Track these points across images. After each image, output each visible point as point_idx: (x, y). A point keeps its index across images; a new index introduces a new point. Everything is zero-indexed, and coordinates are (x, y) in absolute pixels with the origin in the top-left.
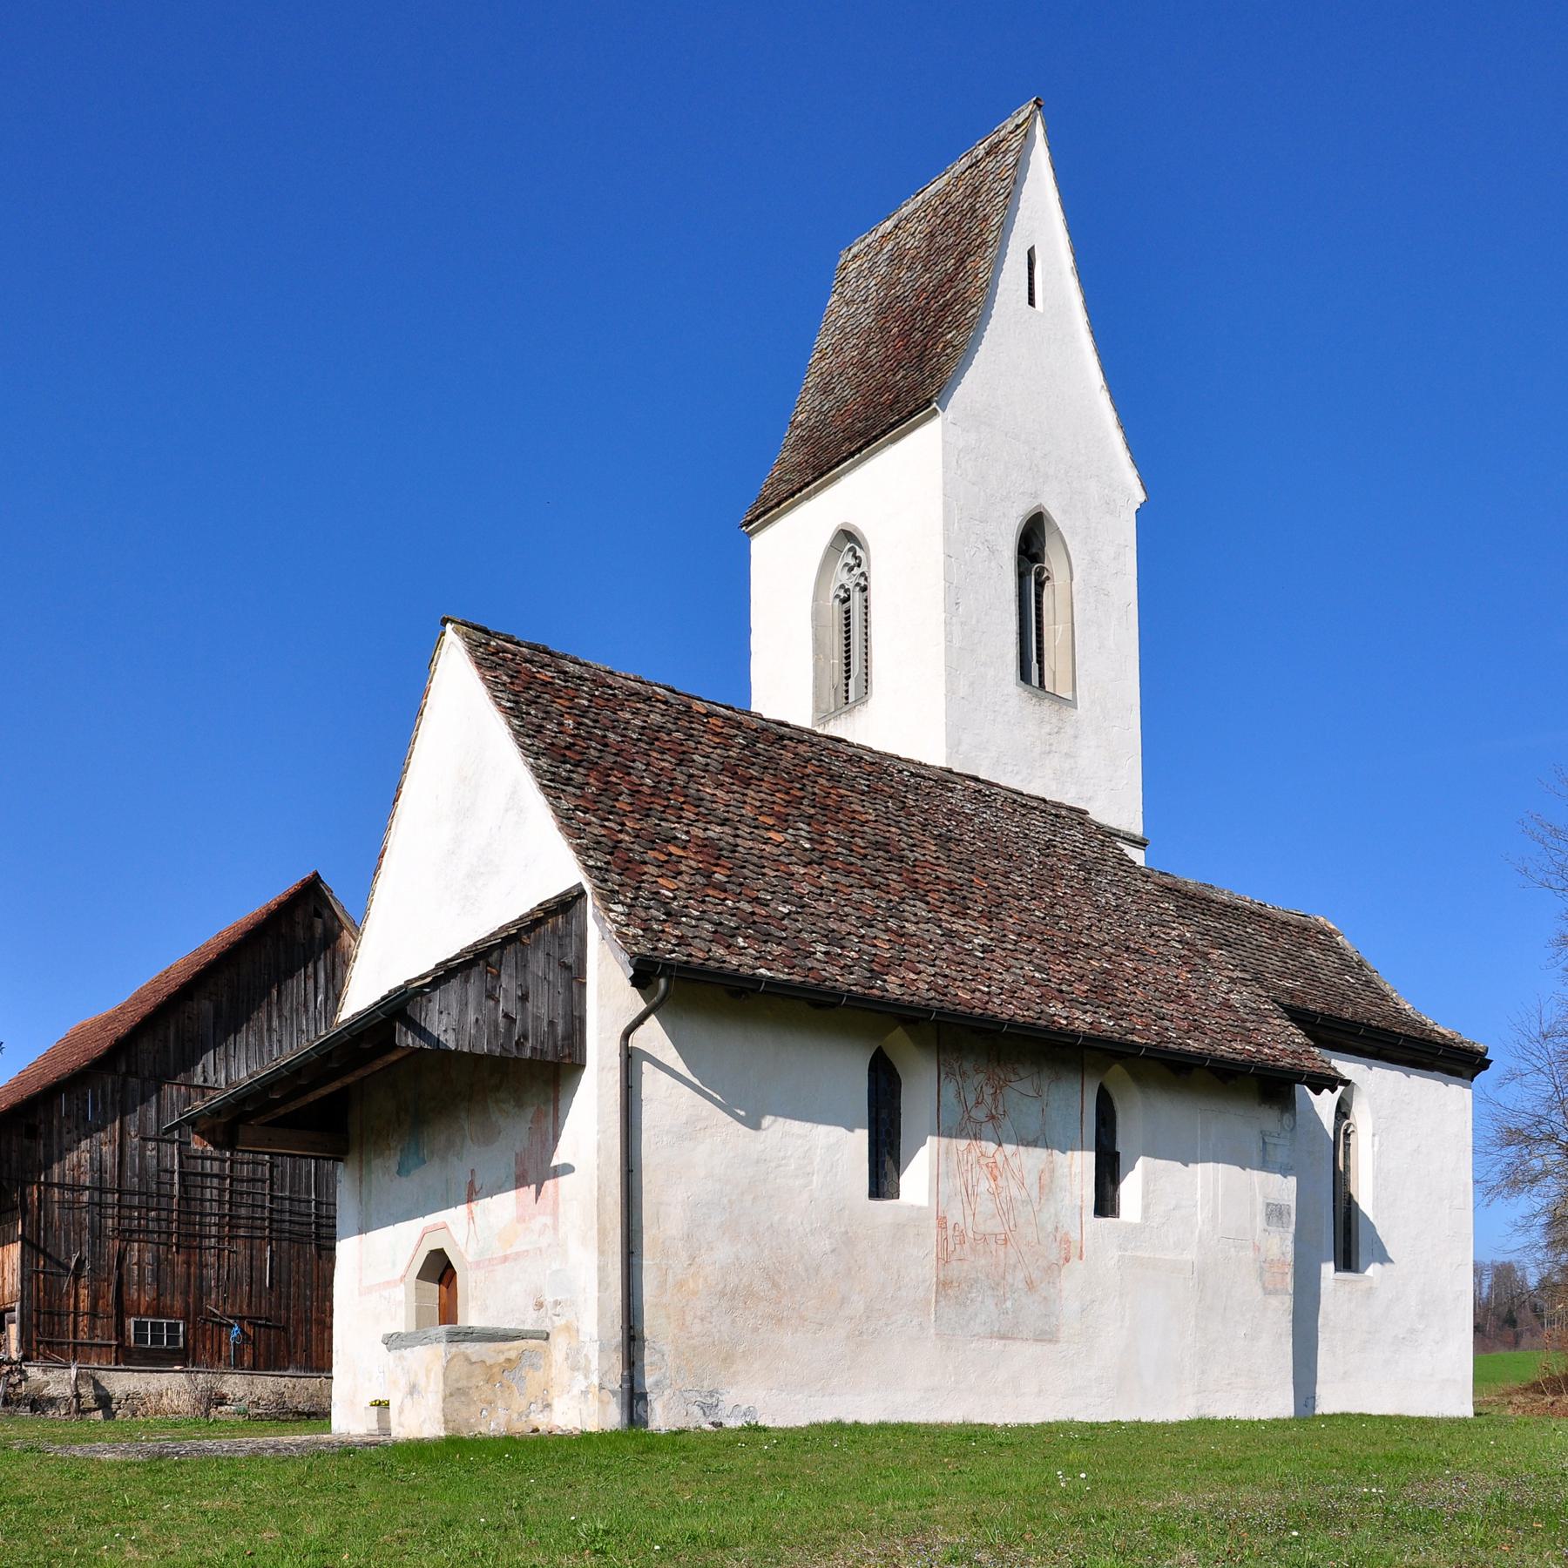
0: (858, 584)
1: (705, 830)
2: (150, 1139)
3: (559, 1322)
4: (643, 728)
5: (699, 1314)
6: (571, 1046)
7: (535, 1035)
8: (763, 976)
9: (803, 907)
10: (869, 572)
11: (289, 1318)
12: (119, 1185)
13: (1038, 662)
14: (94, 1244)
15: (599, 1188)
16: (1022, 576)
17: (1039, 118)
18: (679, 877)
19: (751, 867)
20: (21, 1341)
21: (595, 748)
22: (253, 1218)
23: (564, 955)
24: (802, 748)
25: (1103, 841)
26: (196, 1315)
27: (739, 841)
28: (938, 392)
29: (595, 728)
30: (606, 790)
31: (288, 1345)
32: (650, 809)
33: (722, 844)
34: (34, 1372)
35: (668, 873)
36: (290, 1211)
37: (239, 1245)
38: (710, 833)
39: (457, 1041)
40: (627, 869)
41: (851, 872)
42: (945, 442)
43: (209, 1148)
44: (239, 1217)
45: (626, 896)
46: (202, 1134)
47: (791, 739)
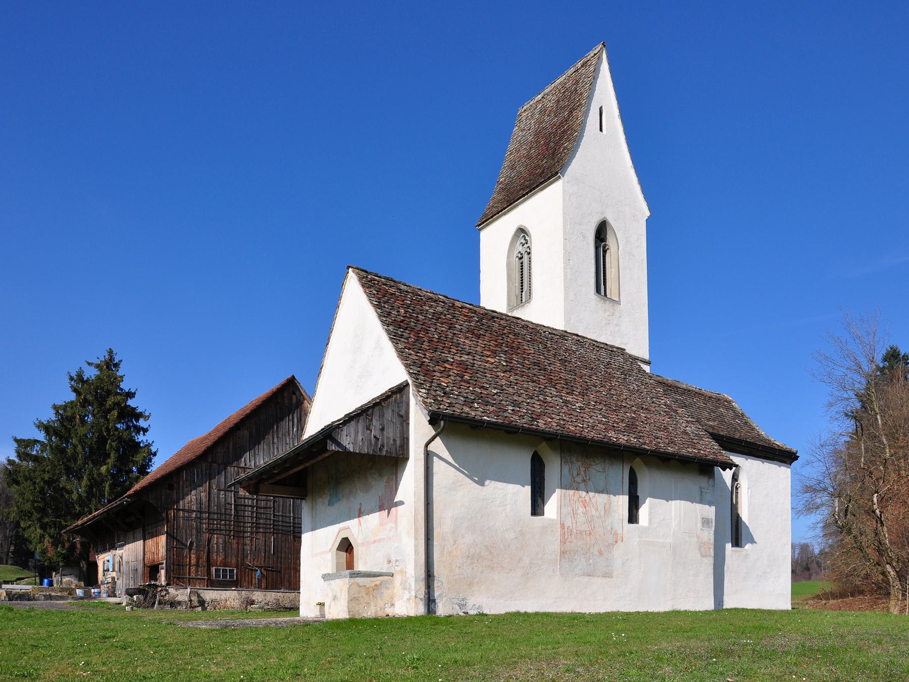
0: (526, 251)
1: (461, 357)
2: (221, 490)
3: (398, 569)
4: (434, 313)
5: (458, 565)
6: (403, 450)
7: (387, 445)
8: (486, 420)
9: (503, 390)
10: (531, 246)
11: (281, 567)
12: (208, 510)
13: (604, 285)
14: (197, 535)
15: (415, 511)
16: (597, 248)
17: (604, 51)
18: (449, 378)
19: (480, 373)
20: (166, 577)
21: (413, 322)
22: (266, 524)
23: (400, 411)
24: (502, 322)
25: (632, 362)
26: (241, 566)
27: (475, 362)
28: (561, 168)
29: (413, 313)
30: (418, 340)
31: (281, 579)
32: (437, 348)
33: (468, 363)
34: (172, 590)
35: (445, 376)
36: (282, 521)
37: (260, 536)
38: (463, 359)
39: (354, 448)
40: (427, 374)
41: (523, 375)
42: (564, 190)
43: (247, 494)
44: (260, 524)
45: (427, 386)
46: (244, 488)
47: (497, 318)
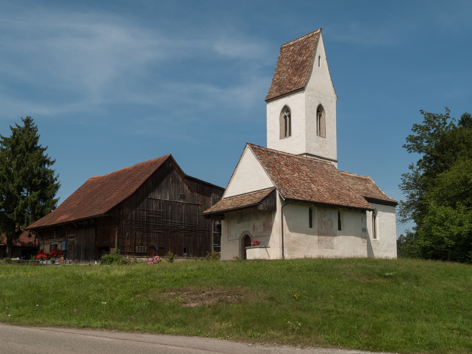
16: (317, 115)
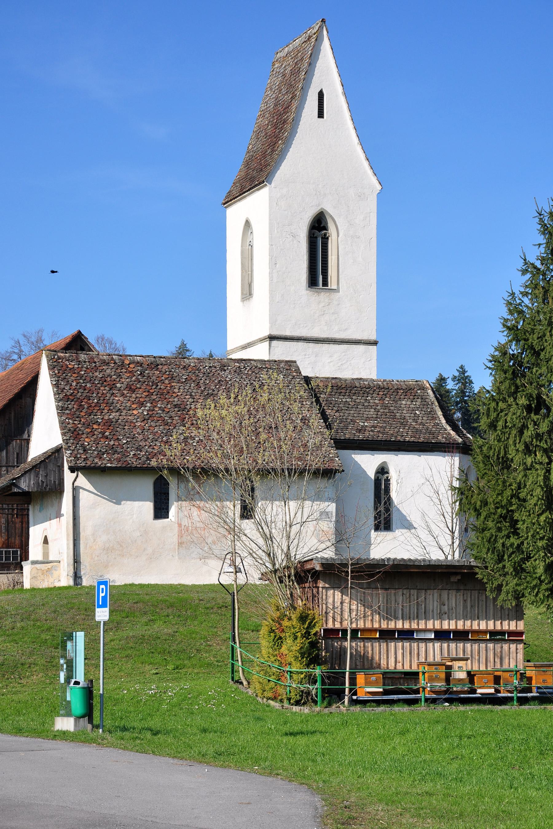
7: (50, 485)
39: (28, 489)
